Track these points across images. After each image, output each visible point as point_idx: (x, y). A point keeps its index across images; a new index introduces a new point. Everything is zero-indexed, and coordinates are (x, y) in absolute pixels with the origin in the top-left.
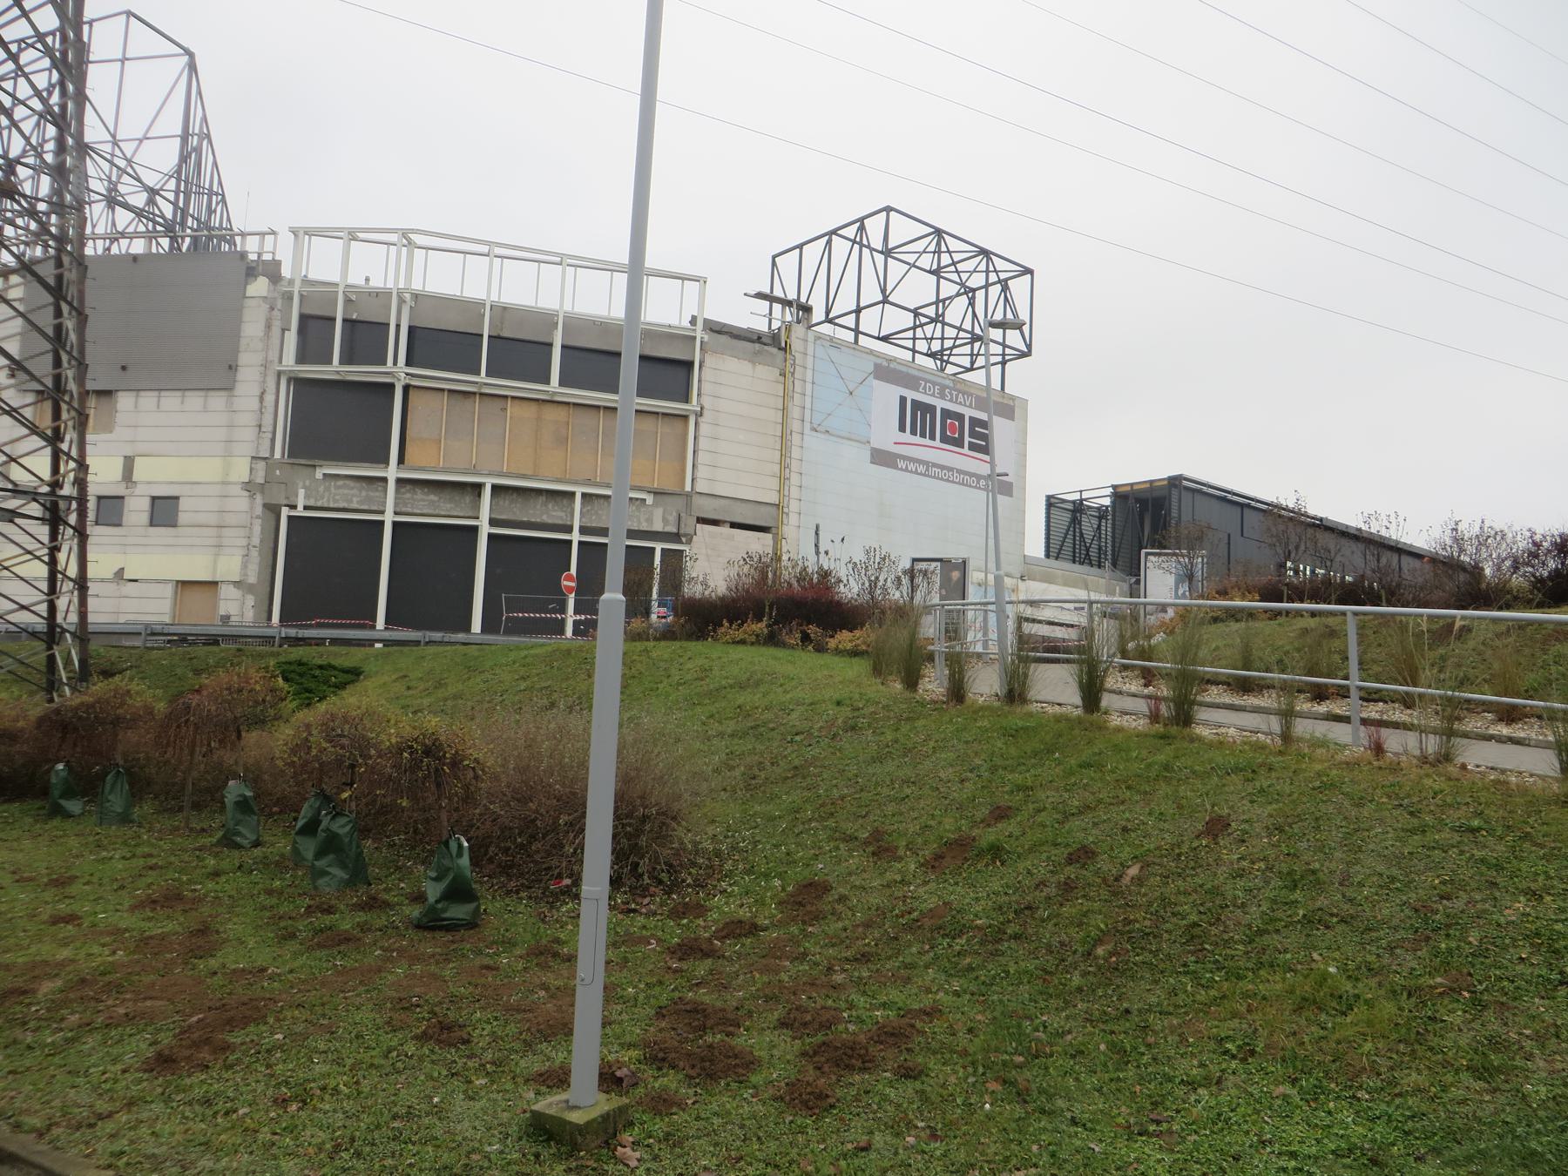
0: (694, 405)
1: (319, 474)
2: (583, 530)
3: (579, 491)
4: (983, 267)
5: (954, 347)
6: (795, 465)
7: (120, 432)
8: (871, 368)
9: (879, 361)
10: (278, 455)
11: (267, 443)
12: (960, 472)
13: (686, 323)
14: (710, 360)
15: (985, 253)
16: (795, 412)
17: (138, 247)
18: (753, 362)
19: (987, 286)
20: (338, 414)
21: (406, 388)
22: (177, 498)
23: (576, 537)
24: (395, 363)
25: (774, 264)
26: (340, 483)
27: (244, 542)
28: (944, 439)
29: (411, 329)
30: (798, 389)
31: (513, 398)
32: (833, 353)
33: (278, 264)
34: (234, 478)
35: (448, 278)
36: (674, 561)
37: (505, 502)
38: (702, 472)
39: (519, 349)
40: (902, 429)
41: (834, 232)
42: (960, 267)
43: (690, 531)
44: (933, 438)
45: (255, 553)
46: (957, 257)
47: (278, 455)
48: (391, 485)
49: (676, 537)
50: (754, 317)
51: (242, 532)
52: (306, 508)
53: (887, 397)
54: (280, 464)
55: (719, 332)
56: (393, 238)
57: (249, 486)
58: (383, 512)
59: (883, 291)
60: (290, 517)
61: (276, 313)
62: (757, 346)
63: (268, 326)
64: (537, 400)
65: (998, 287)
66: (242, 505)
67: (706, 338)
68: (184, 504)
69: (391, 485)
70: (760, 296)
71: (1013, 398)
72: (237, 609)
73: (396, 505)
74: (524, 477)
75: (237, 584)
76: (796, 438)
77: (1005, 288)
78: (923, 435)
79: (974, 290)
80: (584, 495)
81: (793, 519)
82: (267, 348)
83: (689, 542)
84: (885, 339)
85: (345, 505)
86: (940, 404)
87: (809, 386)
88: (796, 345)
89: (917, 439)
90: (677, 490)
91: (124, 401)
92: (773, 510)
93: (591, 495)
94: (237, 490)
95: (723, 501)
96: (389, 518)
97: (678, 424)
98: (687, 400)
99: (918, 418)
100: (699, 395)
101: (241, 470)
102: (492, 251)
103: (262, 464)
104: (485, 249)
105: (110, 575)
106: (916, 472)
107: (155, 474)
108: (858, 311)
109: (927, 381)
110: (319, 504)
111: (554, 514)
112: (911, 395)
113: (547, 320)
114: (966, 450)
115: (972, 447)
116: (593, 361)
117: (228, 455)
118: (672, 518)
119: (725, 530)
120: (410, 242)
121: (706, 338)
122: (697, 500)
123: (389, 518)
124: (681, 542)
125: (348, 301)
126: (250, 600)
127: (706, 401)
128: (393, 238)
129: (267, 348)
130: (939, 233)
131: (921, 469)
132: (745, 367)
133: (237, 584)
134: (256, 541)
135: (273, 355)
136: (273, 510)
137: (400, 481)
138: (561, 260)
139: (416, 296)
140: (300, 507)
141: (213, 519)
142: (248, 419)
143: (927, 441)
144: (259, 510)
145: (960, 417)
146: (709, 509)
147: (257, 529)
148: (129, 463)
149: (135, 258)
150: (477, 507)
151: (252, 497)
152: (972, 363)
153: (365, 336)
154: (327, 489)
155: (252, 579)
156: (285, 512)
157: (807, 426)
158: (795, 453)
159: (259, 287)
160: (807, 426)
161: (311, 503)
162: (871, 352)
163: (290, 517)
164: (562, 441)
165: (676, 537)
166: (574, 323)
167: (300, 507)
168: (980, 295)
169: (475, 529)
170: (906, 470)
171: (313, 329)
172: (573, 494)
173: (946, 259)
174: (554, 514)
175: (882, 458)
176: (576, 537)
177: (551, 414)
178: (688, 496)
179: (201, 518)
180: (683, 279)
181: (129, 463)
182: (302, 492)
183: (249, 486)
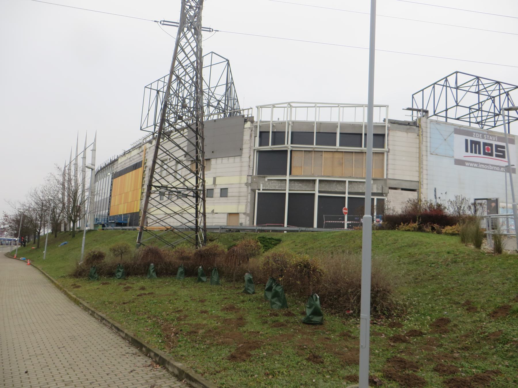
0: (386, 149)
1: (266, 179)
2: (349, 193)
3: (347, 180)
4: (498, 88)
5: (487, 119)
6: (424, 167)
7: (212, 170)
8: (453, 130)
9: (456, 127)
10: (254, 174)
11: (251, 171)
12: (492, 165)
13: (382, 121)
14: (391, 133)
15: (498, 83)
16: (424, 148)
17: (215, 117)
18: (407, 132)
19: (500, 95)
20: (272, 161)
21: (291, 151)
22: (227, 189)
23: (347, 196)
24: (288, 143)
25: (413, 97)
26: (272, 182)
27: (246, 201)
28: (485, 154)
29: (292, 133)
30: (424, 139)
31: (325, 151)
32: (438, 126)
33: (253, 117)
34: (242, 182)
35: (303, 116)
36: (381, 202)
37: (323, 185)
38: (390, 171)
39: (326, 136)
40: (467, 151)
41: (435, 83)
42: (487, 89)
43: (386, 192)
44: (480, 153)
45: (249, 204)
46: (486, 86)
47: (254, 174)
48: (288, 182)
49: (381, 194)
50: (407, 117)
51: (245, 198)
52: (263, 190)
53: (460, 140)
54: (255, 177)
55: (394, 123)
56: (286, 105)
57: (247, 184)
58: (285, 190)
59: (456, 102)
60: (258, 193)
61: (253, 132)
62: (408, 127)
63: (251, 136)
64: (332, 151)
65: (505, 95)
66: (245, 190)
67: (389, 125)
68: (229, 190)
69: (288, 182)
70: (409, 109)
71: (514, 136)
72: (244, 221)
73: (289, 187)
74: (329, 177)
75: (244, 214)
76: (424, 158)
77: (508, 95)
78: (476, 153)
79: (494, 97)
80: (349, 182)
81: (425, 186)
82: (251, 143)
83: (386, 196)
84: (458, 119)
85: (273, 188)
86: (482, 141)
87: (429, 139)
88: (423, 125)
89: (474, 154)
90: (381, 178)
91: (213, 161)
92: (417, 183)
93: (351, 182)
94: (243, 185)
95: (398, 181)
96: (287, 192)
97: (381, 156)
98: (383, 147)
99: (473, 146)
100: (388, 145)
101: (244, 180)
102: (316, 105)
103: (250, 178)
104: (314, 105)
105: (210, 212)
106: (474, 167)
107: (222, 182)
108: (446, 110)
109: (476, 133)
110: (267, 188)
111: (339, 188)
112: (470, 138)
113: (335, 125)
114: (494, 157)
115: (497, 156)
116: (352, 137)
117: (241, 175)
118: (380, 188)
119: (400, 191)
120: (291, 106)
121: (389, 125)
122: (389, 181)
123: (287, 192)
124: (383, 196)
125: (273, 126)
126: (248, 218)
127: (390, 147)
128: (286, 105)
129: (251, 143)
130: (478, 78)
131: (476, 165)
132: (404, 134)
133: (244, 214)
134: (249, 200)
135: (253, 145)
136: (254, 191)
137: (290, 180)
138: (338, 105)
139: (293, 122)
140: (261, 190)
141: (237, 194)
142: (246, 164)
143: (478, 155)
144: (250, 191)
145: (491, 145)
146: (393, 184)
147: (249, 197)
148: (215, 179)
149: (215, 120)
150: (314, 187)
151: (248, 187)
152: (495, 124)
153: (279, 136)
154: (269, 184)
155: (248, 212)
156: (257, 191)
157: (429, 153)
158: (425, 163)
159: (248, 125)
160: (429, 153)
161: (264, 188)
162: (453, 124)
163: (258, 193)
164: (341, 164)
165: (381, 194)
166: (343, 126)
167: (261, 190)
168: (497, 99)
169: (314, 194)
170: (469, 166)
171: (263, 135)
172: (345, 181)
173: (481, 87)
174: (339, 188)
175: (459, 162)
176: (347, 196)
177: (337, 155)
178: (385, 180)
179: (234, 194)
180: (380, 107)
181: (215, 179)
182: (261, 185)
183: (247, 184)
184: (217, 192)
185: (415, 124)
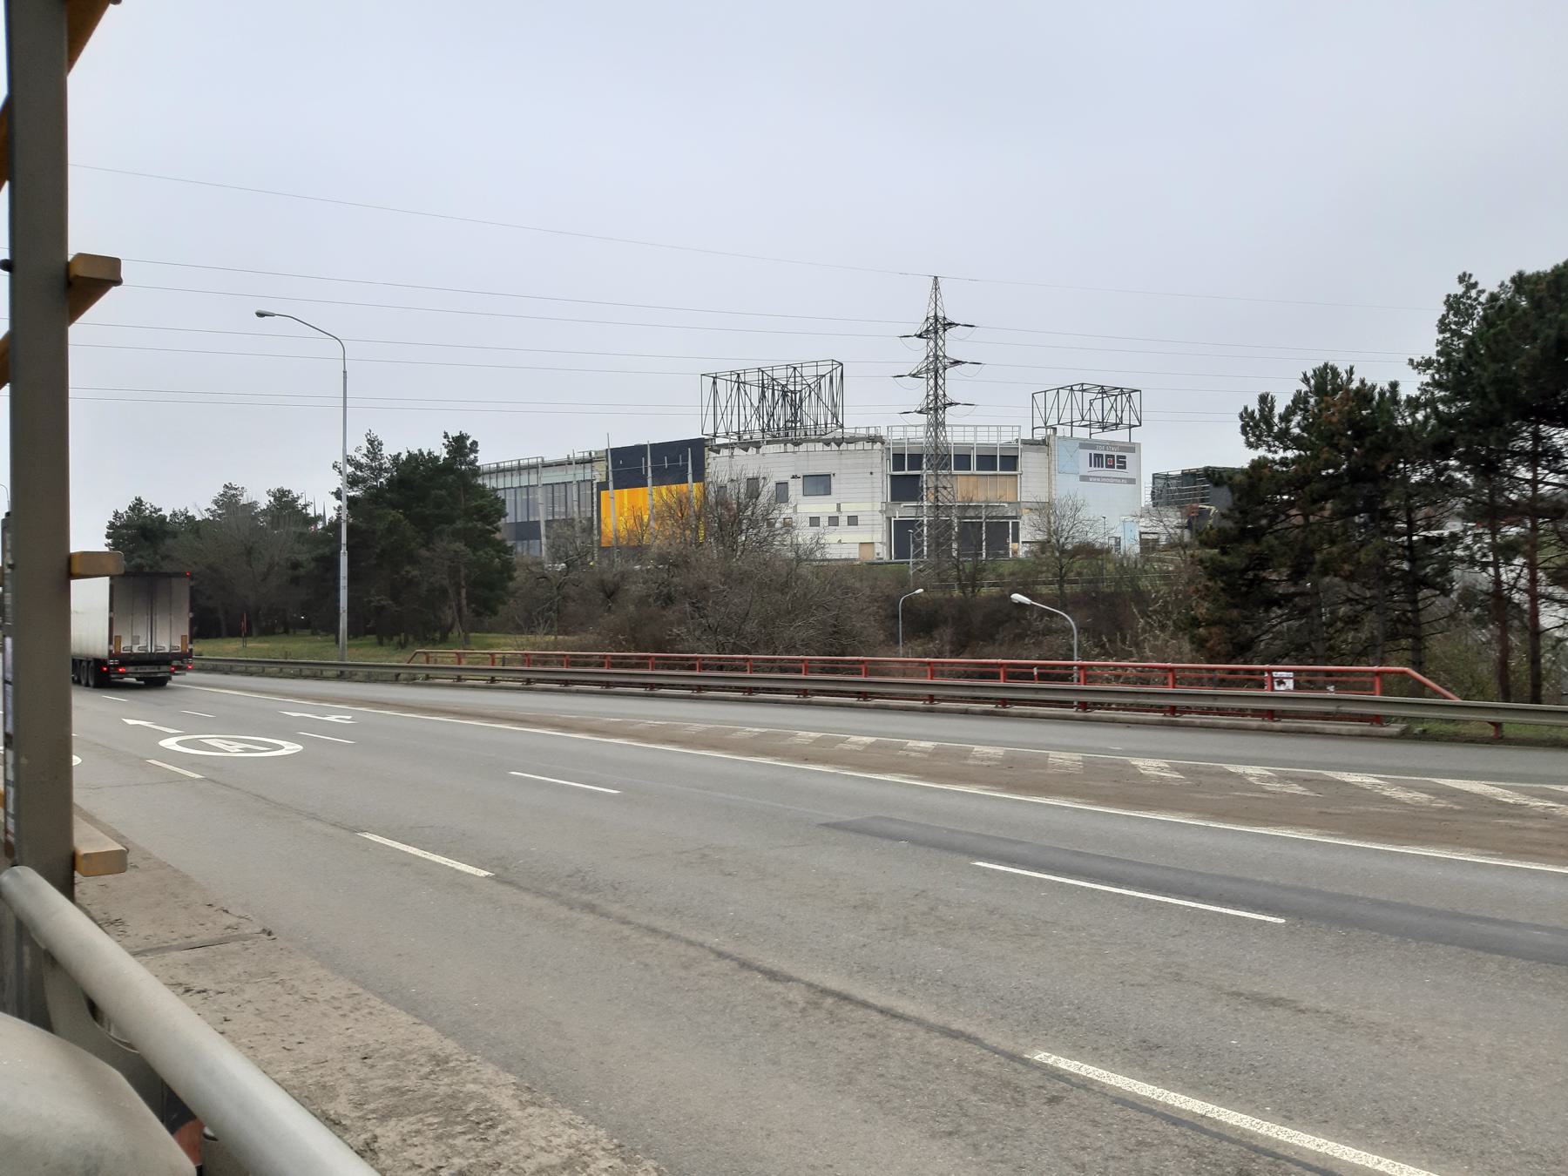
20: (904, 488)
50: (1040, 435)
66: (880, 519)
86: (1105, 453)
99: (1097, 460)
101: (878, 507)
107: (849, 509)
116: (987, 461)
166: (980, 447)
171: (898, 460)
175: (1084, 478)
184: (843, 520)
185: (1044, 443)
